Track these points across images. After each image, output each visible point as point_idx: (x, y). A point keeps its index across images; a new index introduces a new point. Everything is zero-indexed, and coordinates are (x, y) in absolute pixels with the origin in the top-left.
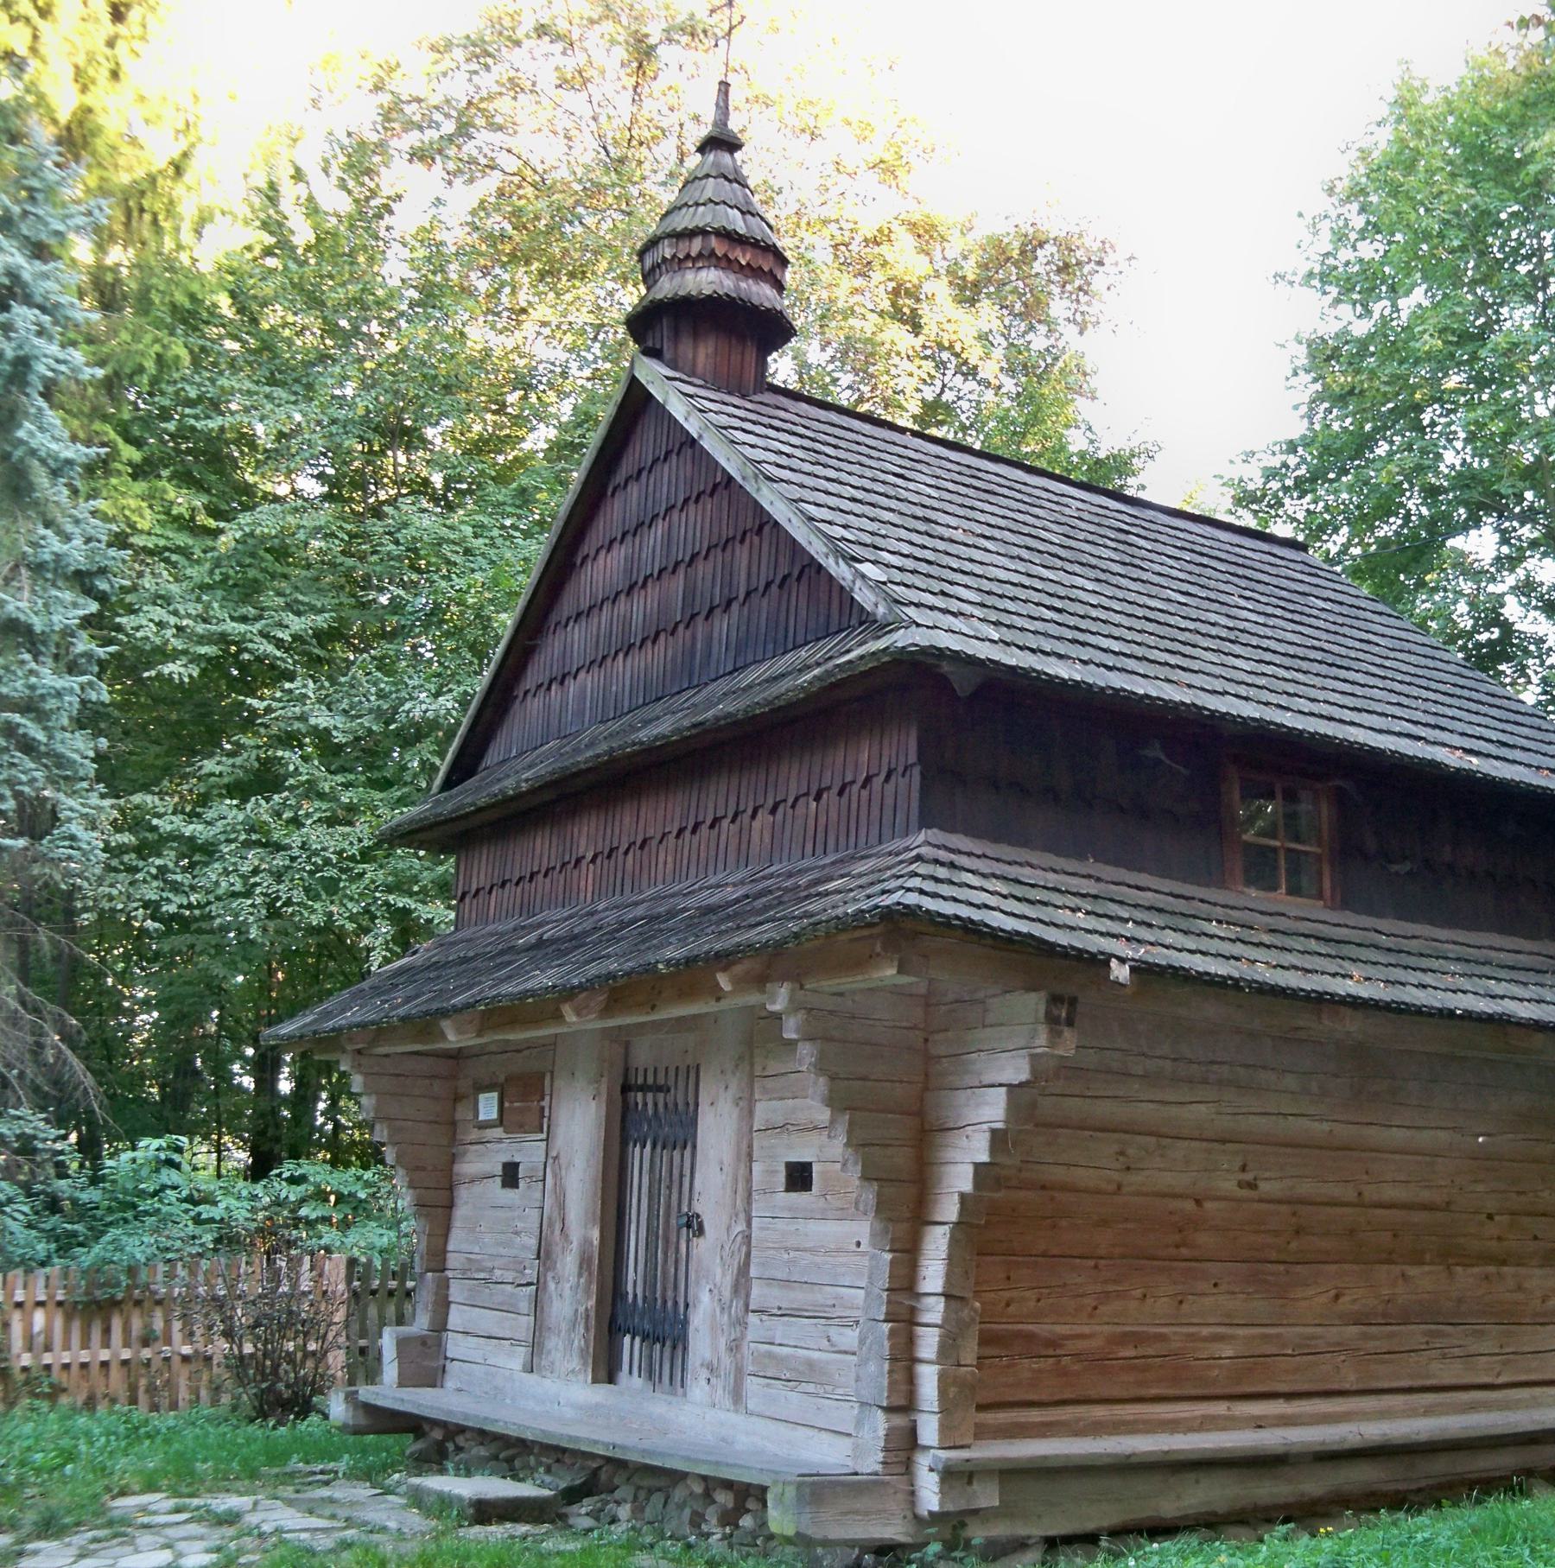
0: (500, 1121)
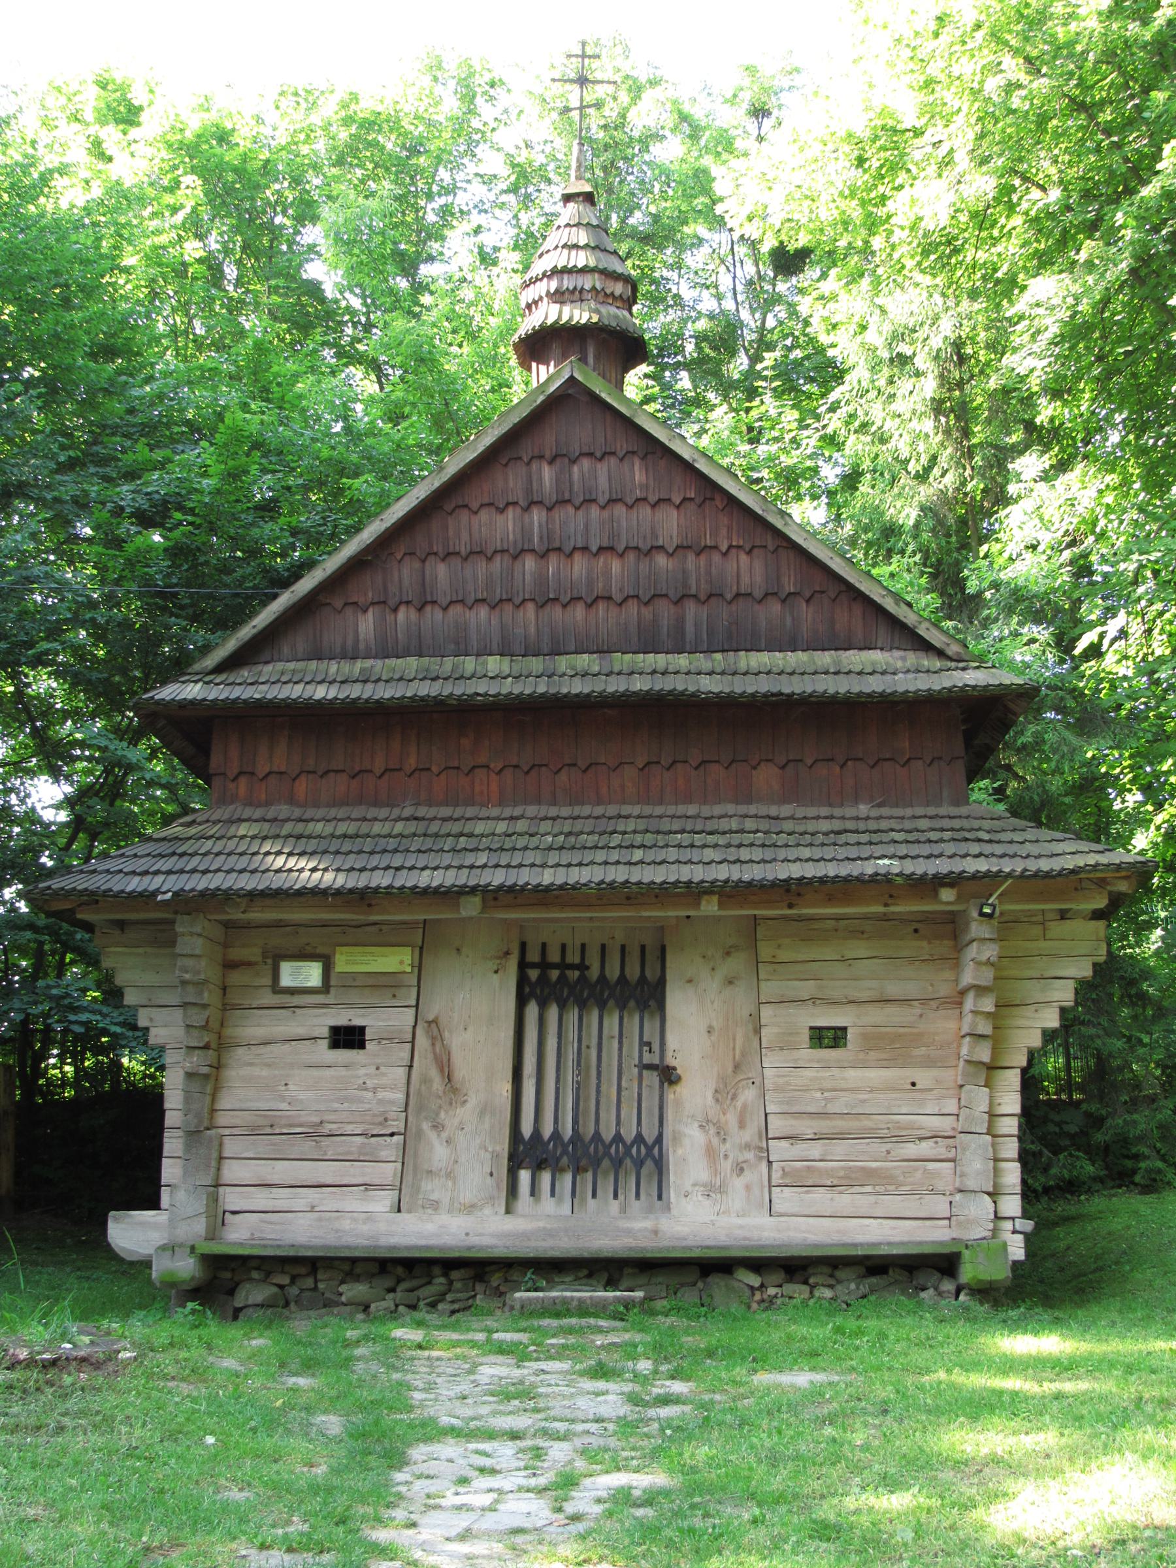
0: (326, 987)
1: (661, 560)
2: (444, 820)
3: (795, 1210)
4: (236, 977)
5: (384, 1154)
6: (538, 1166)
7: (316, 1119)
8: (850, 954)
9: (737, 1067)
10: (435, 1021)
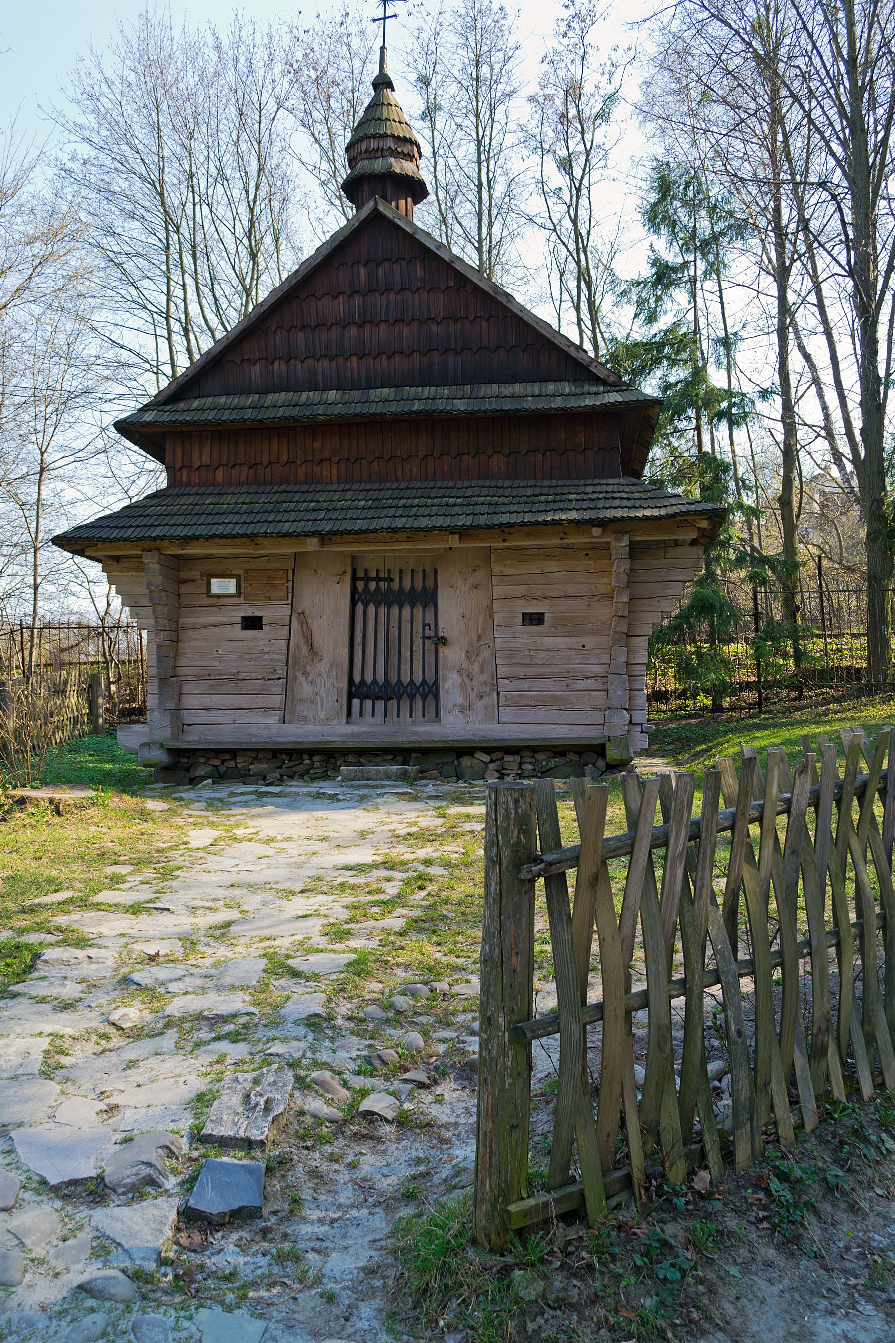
0: (239, 593)
1: (434, 328)
2: (303, 493)
3: (513, 720)
4: (184, 589)
5: (274, 690)
6: (363, 697)
7: (235, 671)
8: (546, 569)
9: (479, 637)
10: (303, 613)
